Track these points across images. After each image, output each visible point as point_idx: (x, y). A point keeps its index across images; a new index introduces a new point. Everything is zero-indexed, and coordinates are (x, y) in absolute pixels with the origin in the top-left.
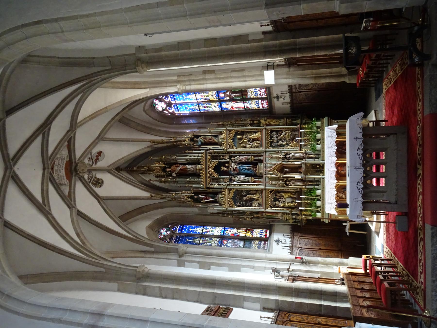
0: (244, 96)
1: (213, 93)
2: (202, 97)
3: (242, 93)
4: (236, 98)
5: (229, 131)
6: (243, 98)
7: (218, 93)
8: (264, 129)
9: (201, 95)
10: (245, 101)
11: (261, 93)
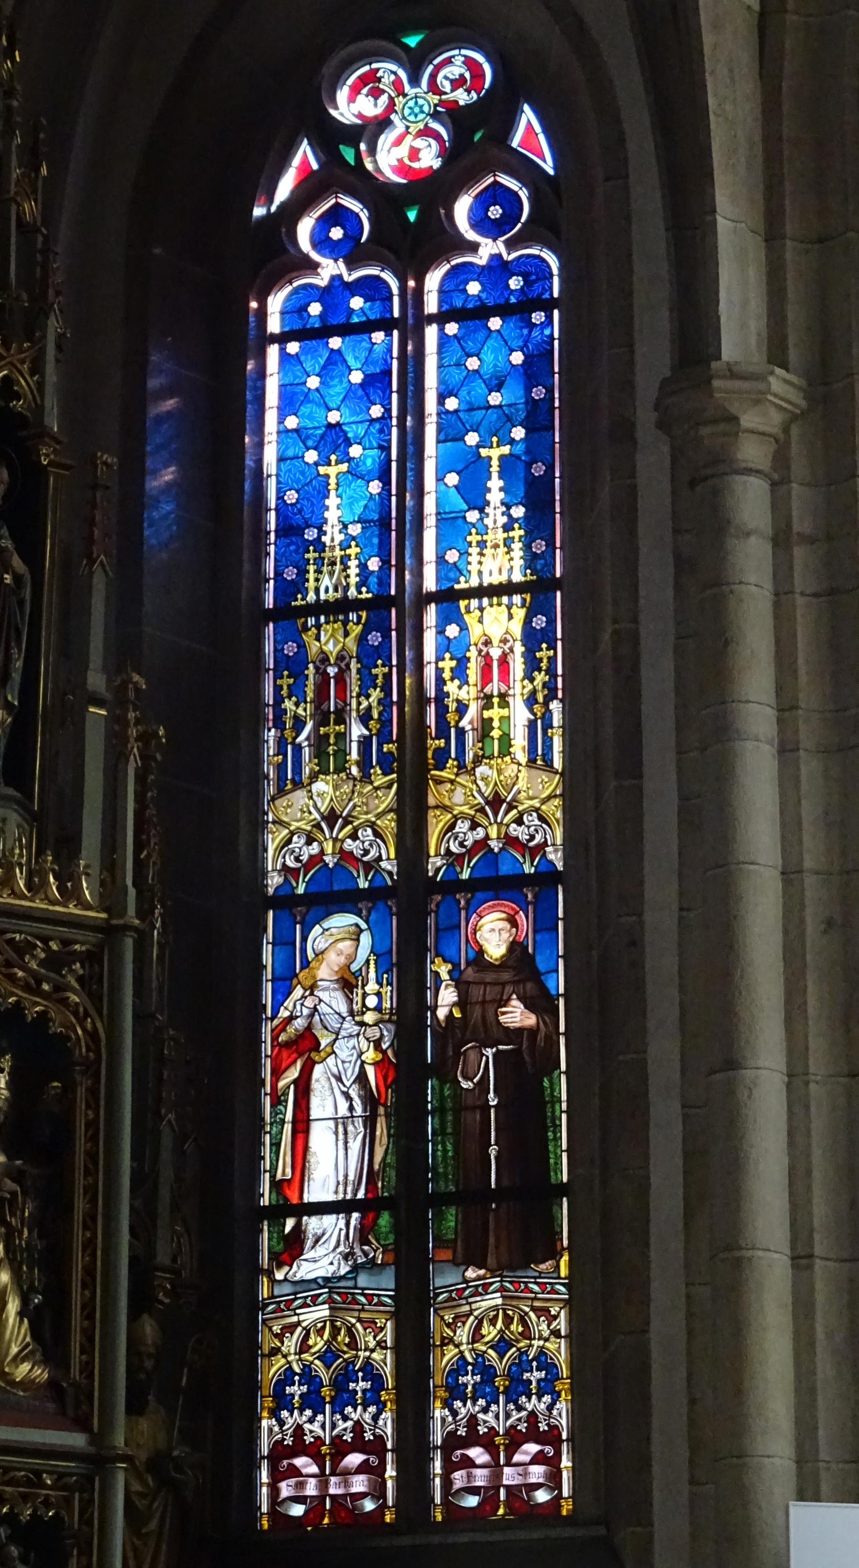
0: (465, 1222)
1: (532, 820)
2: (486, 677)
3: (500, 1194)
4: (440, 1111)
5: (91, 958)
6: (440, 1201)
7: (522, 880)
8: (99, 1439)
9: (518, 666)
10: (385, 1220)
11: (488, 1442)
